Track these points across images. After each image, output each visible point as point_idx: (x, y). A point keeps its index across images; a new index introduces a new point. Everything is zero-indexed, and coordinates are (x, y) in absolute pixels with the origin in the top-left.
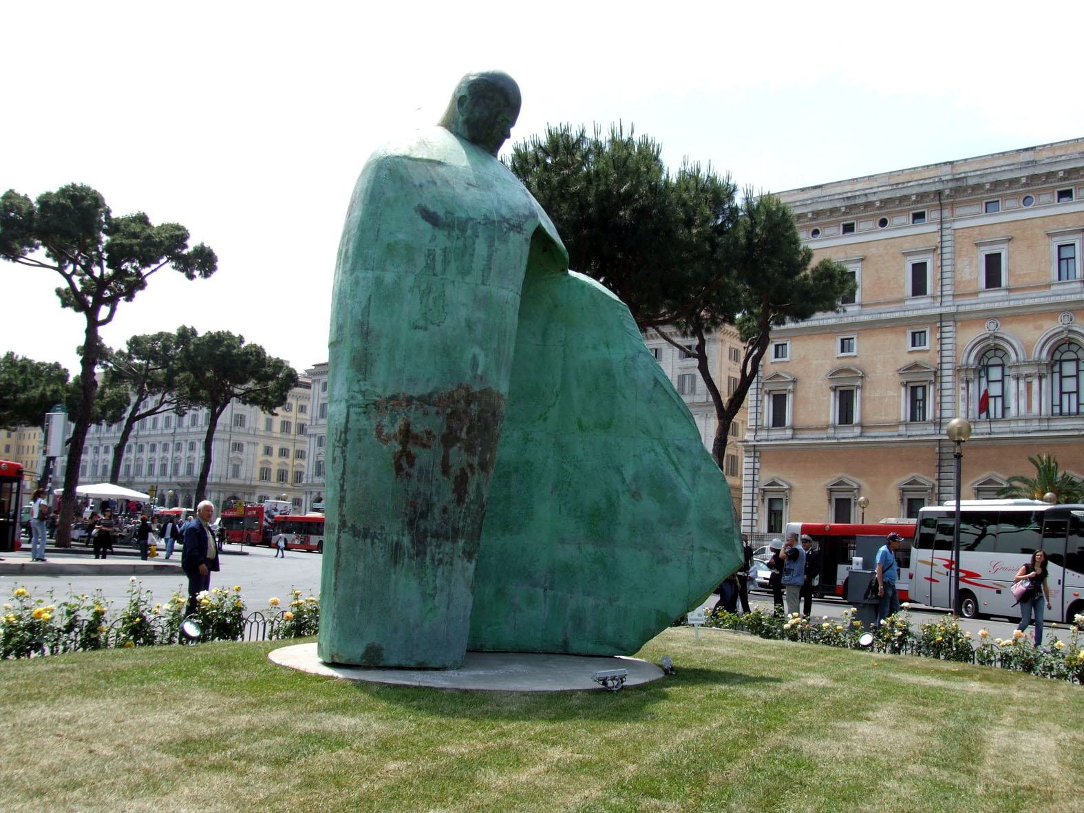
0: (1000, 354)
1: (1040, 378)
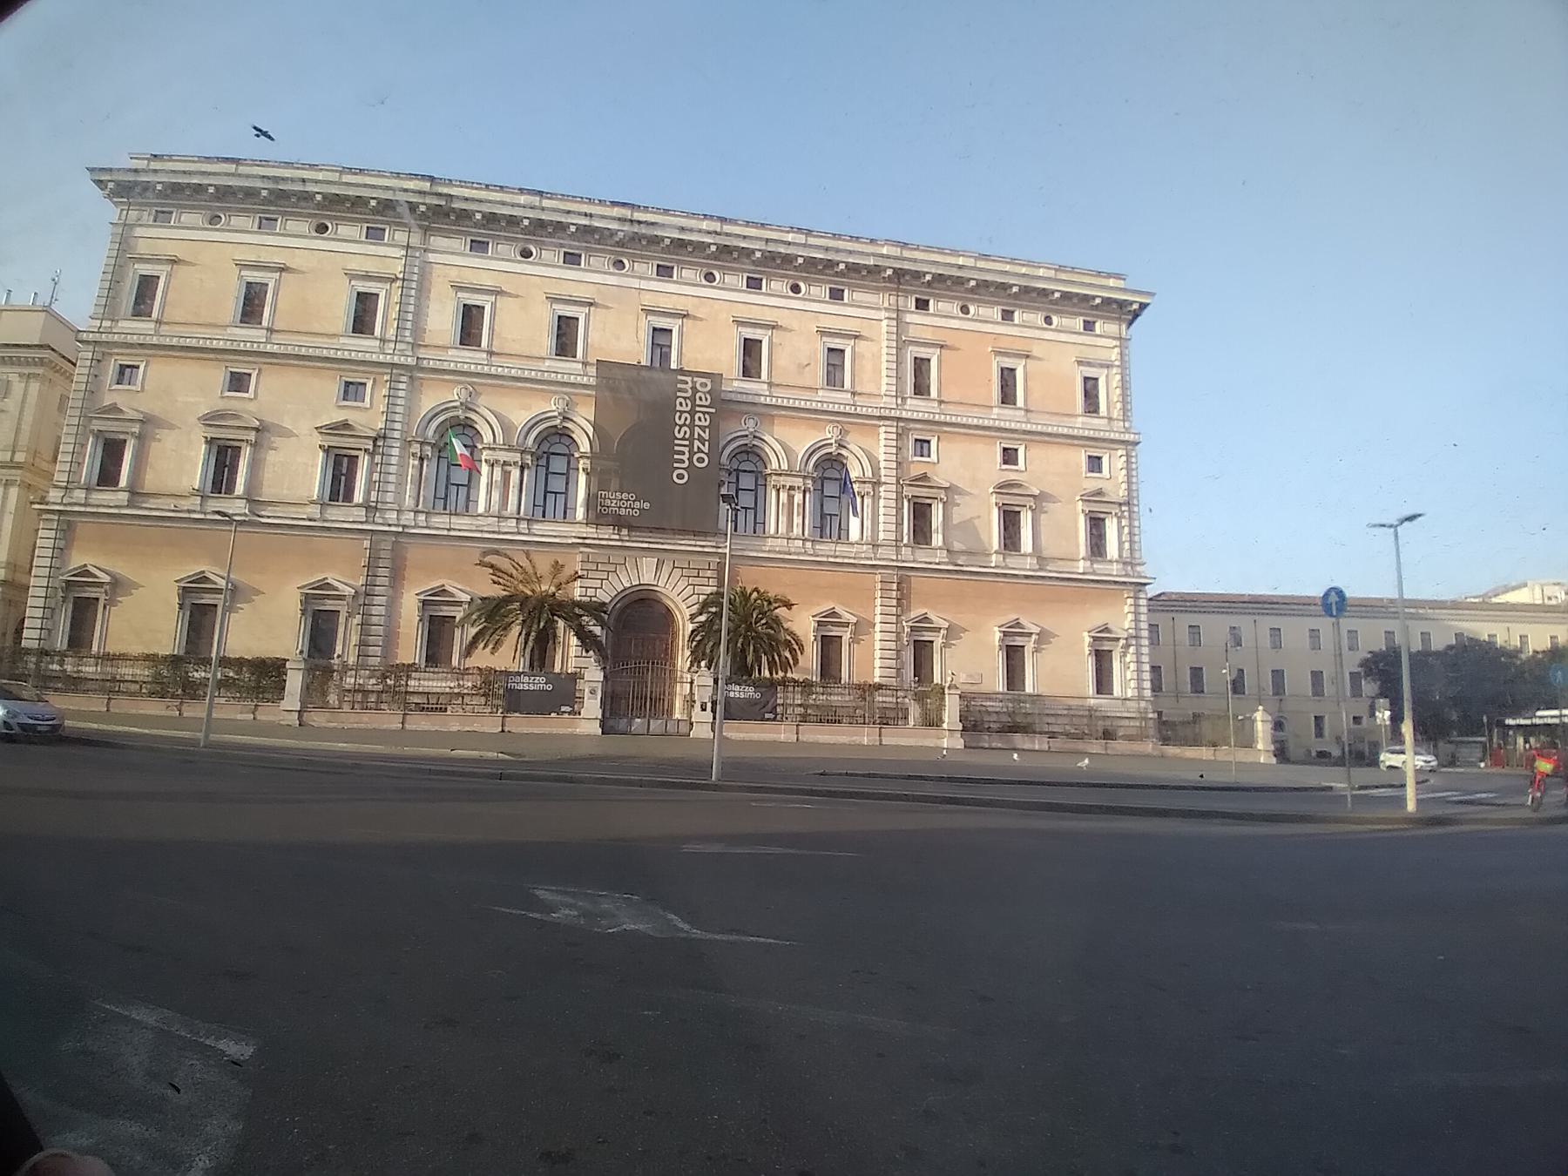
1: (522, 468)
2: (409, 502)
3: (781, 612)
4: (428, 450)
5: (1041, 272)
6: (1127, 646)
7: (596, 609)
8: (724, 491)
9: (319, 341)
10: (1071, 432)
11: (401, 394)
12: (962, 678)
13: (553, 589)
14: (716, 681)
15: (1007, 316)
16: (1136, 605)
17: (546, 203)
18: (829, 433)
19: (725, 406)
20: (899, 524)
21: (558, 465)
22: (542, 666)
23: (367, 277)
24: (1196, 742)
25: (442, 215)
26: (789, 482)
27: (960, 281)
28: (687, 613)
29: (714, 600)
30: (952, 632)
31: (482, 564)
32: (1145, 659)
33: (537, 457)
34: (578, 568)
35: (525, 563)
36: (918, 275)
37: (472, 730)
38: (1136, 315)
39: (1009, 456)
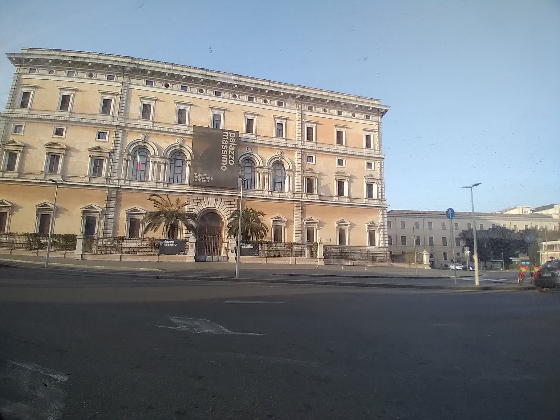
0: (145, 150)
1: (165, 164)
2: (122, 177)
3: (260, 217)
4: (130, 157)
5: (351, 98)
6: (381, 229)
7: (193, 216)
8: (240, 174)
9: (89, 117)
10: (361, 154)
11: (120, 136)
12: (323, 240)
13: (177, 209)
14: (237, 242)
15: (339, 113)
16: (383, 215)
17: (174, 68)
18: (277, 153)
19: (239, 142)
20: (302, 186)
21: (179, 163)
22: (173, 236)
23: (107, 93)
24: (403, 261)
25: (134, 71)
26: (263, 170)
27: (323, 100)
28: (227, 217)
29: (236, 213)
30: (321, 224)
31: (150, 199)
32: (386, 233)
33: (171, 160)
34: (186, 201)
35: (166, 199)
36: (309, 98)
37: (146, 260)
38: (383, 114)
39: (340, 162)
